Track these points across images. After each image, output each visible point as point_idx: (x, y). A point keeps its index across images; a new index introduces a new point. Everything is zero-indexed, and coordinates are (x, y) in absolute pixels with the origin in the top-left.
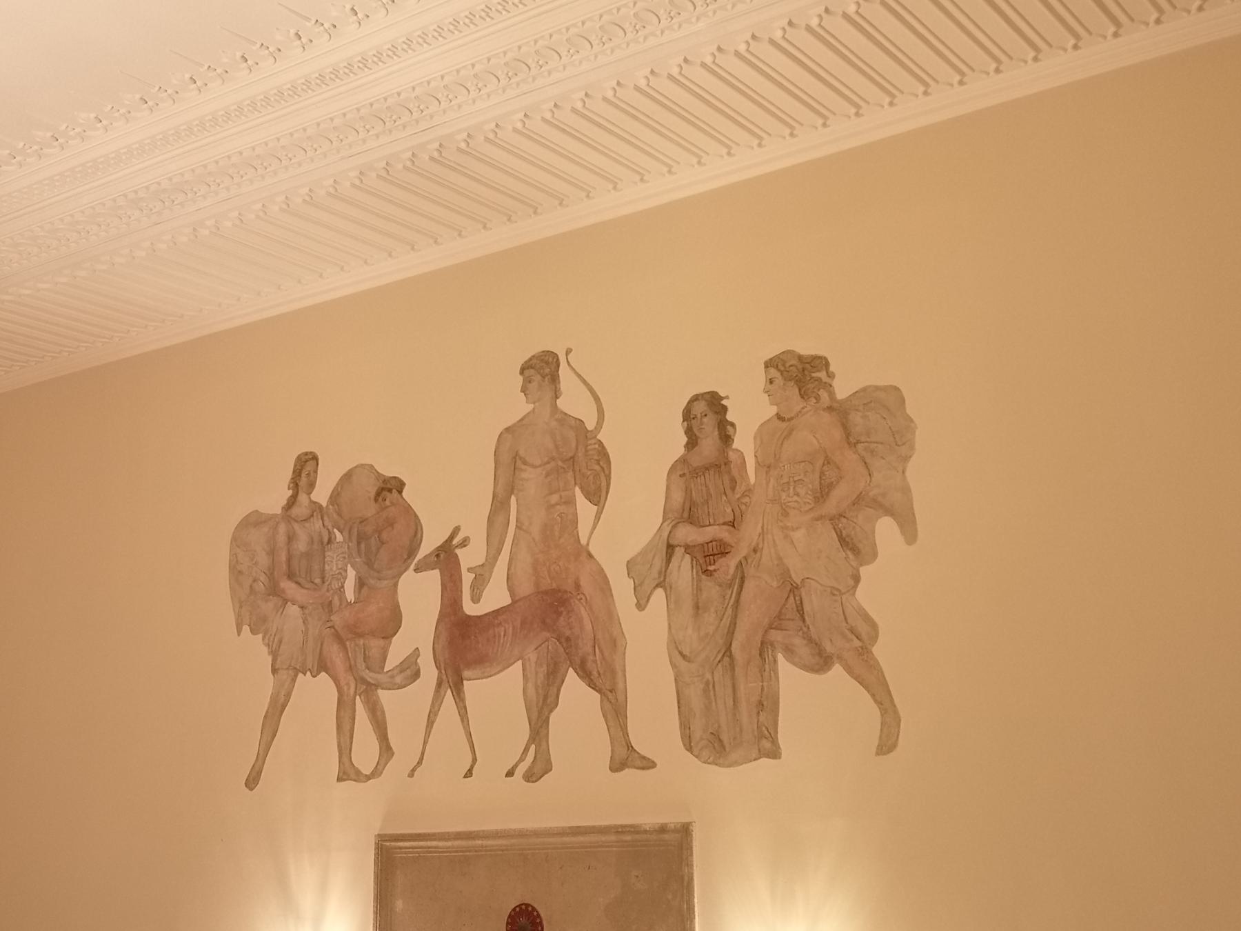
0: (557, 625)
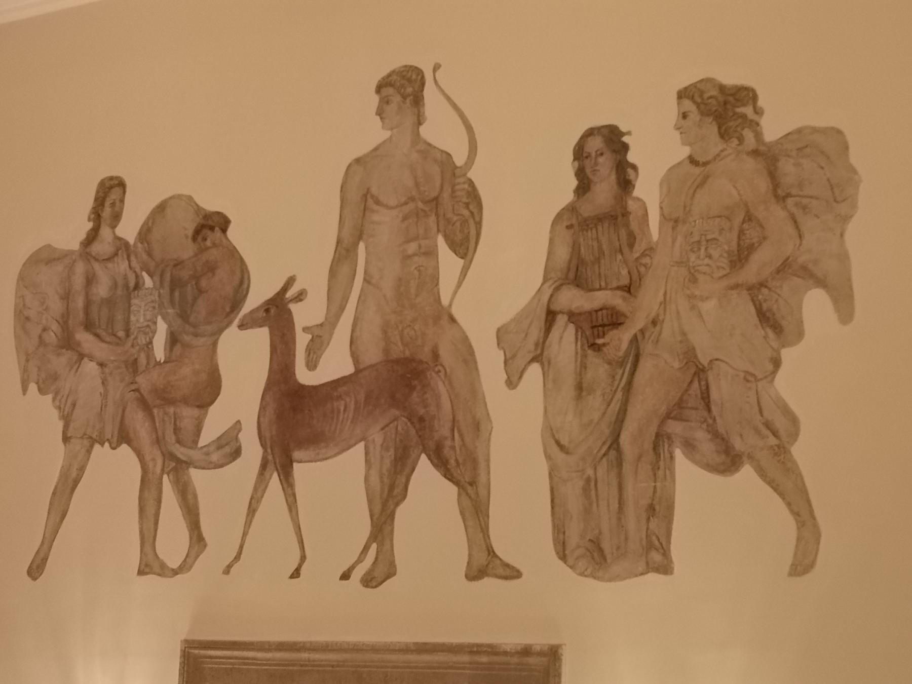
0: (407, 403)
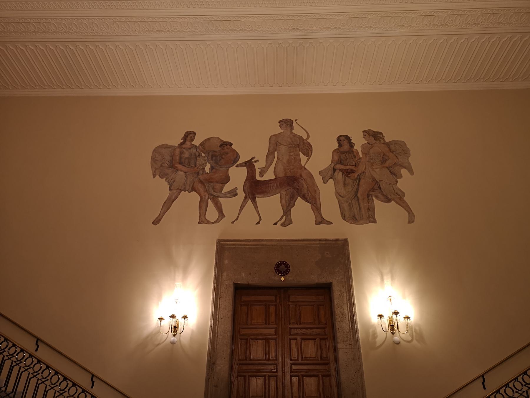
0: (294, 185)
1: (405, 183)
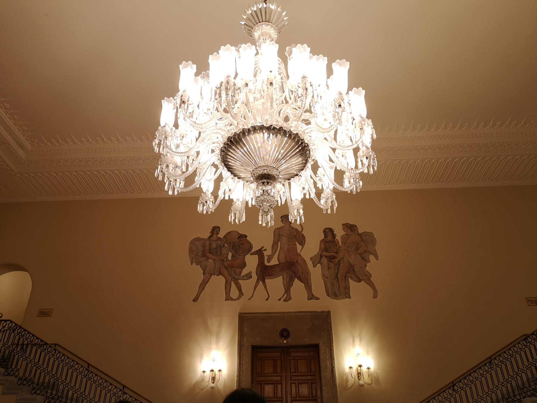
0: (292, 269)
1: (373, 266)
